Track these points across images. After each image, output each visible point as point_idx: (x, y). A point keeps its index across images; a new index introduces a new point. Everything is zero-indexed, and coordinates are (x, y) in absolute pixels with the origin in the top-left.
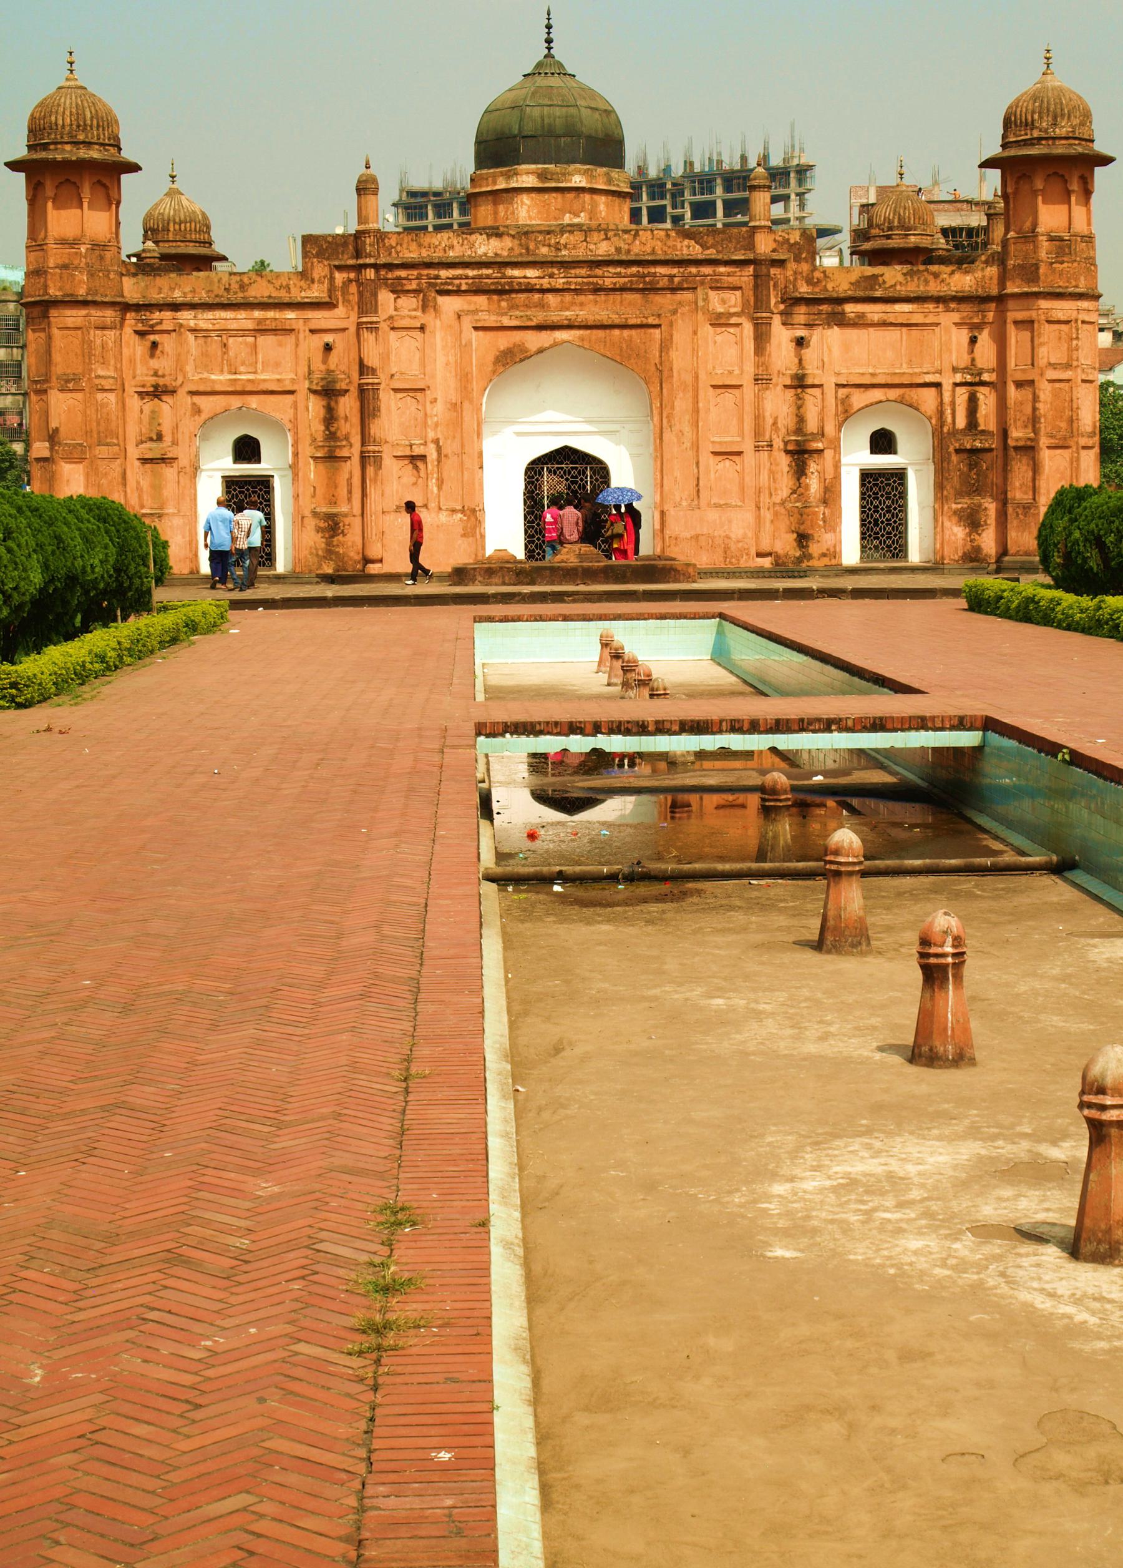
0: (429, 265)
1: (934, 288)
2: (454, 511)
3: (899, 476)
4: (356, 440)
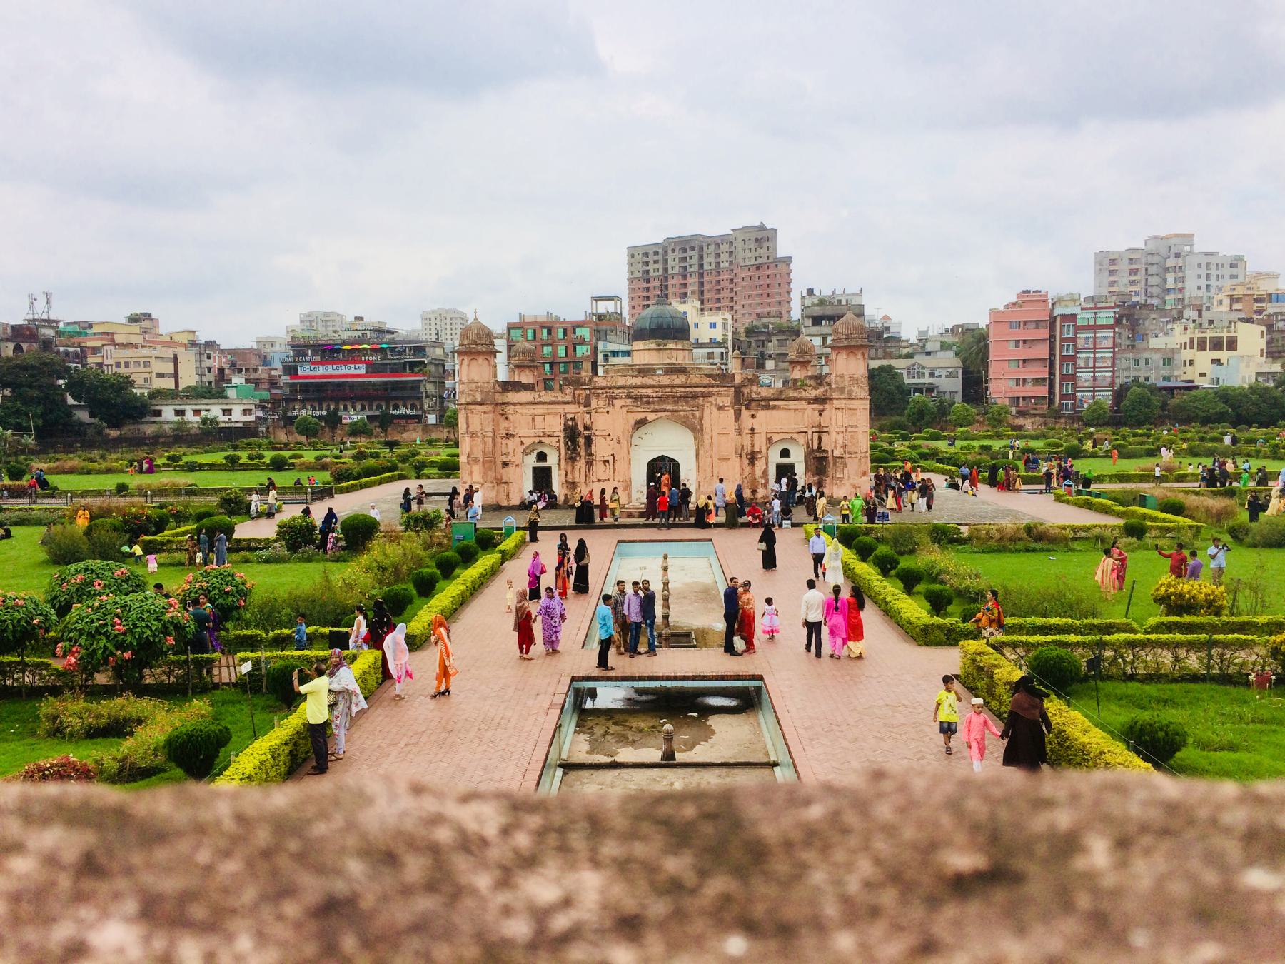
1: (804, 394)
3: (792, 466)
4: (583, 454)
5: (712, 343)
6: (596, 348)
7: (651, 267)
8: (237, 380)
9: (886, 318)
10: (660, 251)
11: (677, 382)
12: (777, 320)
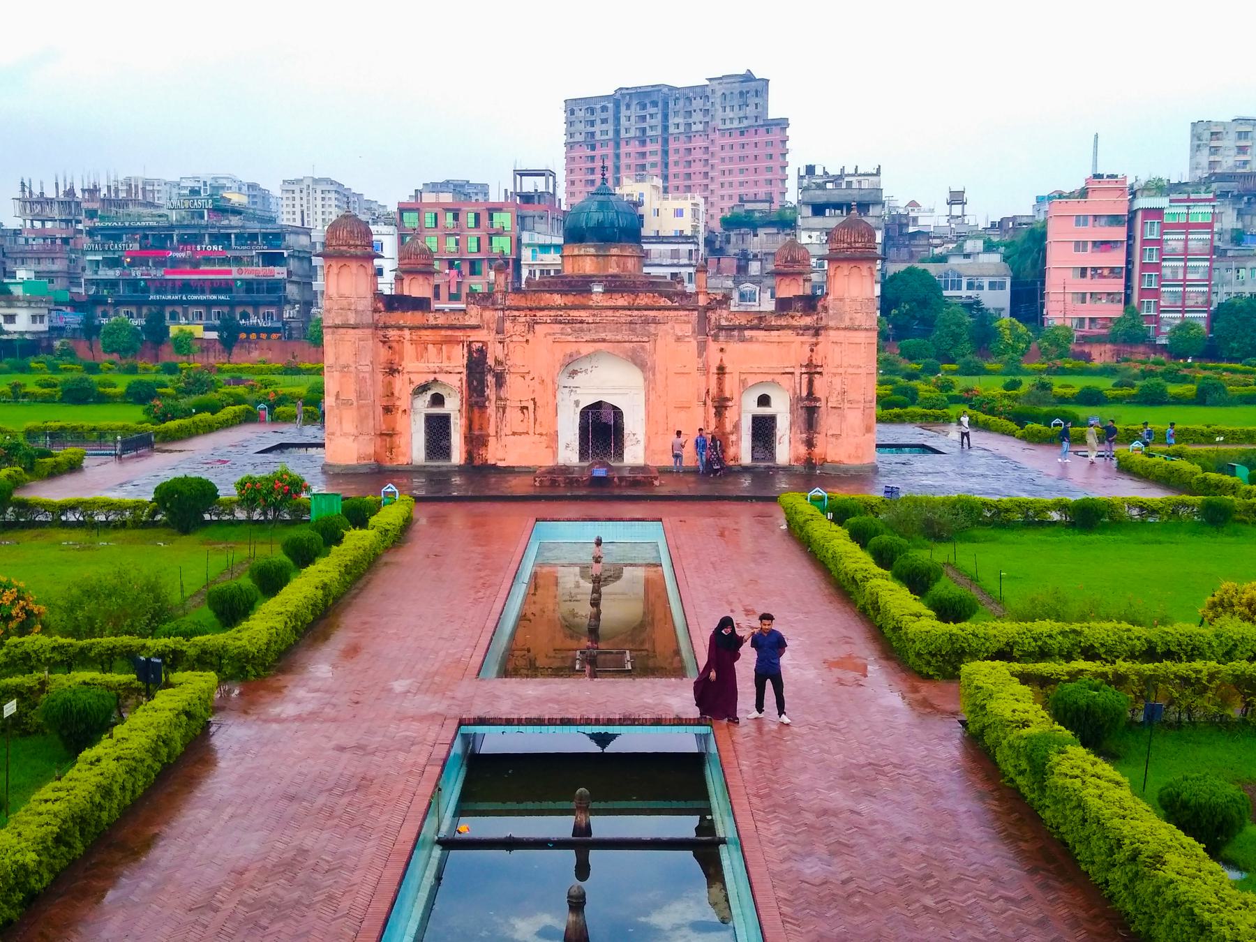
0: (530, 310)
2: (541, 434)
3: (772, 419)
5: (681, 238)
6: (519, 240)
7: (597, 128)
8: (22, 274)
9: (913, 204)
11: (621, 302)
12: (765, 206)
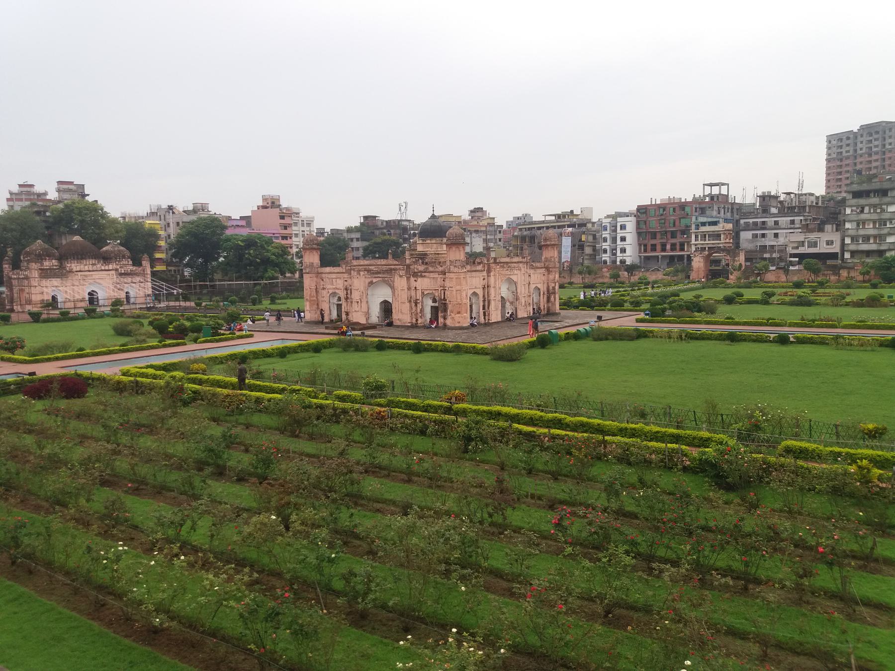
7: (843, 150)
10: (851, 136)
